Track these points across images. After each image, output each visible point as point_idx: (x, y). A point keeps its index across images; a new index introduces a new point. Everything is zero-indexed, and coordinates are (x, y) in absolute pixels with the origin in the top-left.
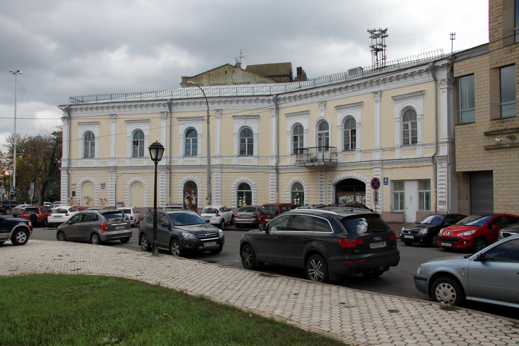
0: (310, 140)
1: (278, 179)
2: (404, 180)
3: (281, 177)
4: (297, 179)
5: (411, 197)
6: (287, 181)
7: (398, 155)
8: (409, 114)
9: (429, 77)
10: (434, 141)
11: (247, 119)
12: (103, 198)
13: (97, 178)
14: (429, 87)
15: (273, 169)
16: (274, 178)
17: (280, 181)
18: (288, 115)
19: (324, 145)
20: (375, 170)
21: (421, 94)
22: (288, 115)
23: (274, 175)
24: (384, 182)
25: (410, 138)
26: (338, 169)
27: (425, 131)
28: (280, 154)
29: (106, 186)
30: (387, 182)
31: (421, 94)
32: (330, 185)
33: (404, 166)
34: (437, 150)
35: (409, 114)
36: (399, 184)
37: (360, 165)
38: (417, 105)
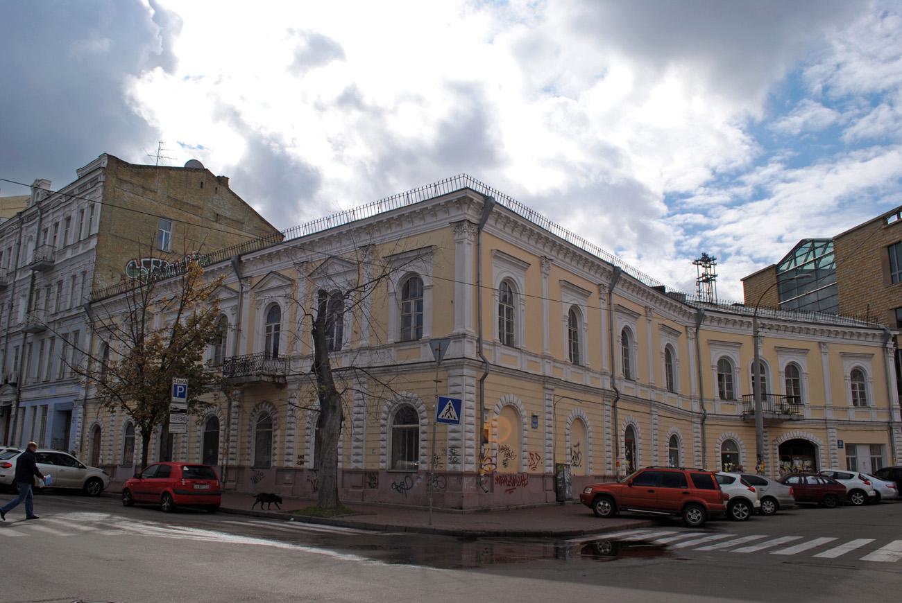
0: (743, 385)
1: (703, 434)
2: (856, 444)
3: (708, 429)
4: (730, 435)
5: (864, 463)
6: (717, 436)
7: (853, 415)
8: (857, 374)
9: (878, 342)
10: (885, 406)
11: (670, 333)
12: (533, 450)
13: (527, 398)
14: (878, 353)
15: (698, 417)
16: (699, 430)
17: (707, 436)
18: (712, 342)
19: (761, 391)
20: (830, 430)
21: (869, 356)
22: (712, 342)
23: (699, 426)
24: (839, 445)
25: (860, 399)
26: (784, 426)
27: (874, 392)
28: (705, 396)
29: (540, 422)
30: (842, 445)
31: (869, 356)
32: (775, 445)
33: (858, 428)
34: (891, 415)
35: (857, 374)
36: (851, 448)
37: (813, 423)
38: (866, 365)
